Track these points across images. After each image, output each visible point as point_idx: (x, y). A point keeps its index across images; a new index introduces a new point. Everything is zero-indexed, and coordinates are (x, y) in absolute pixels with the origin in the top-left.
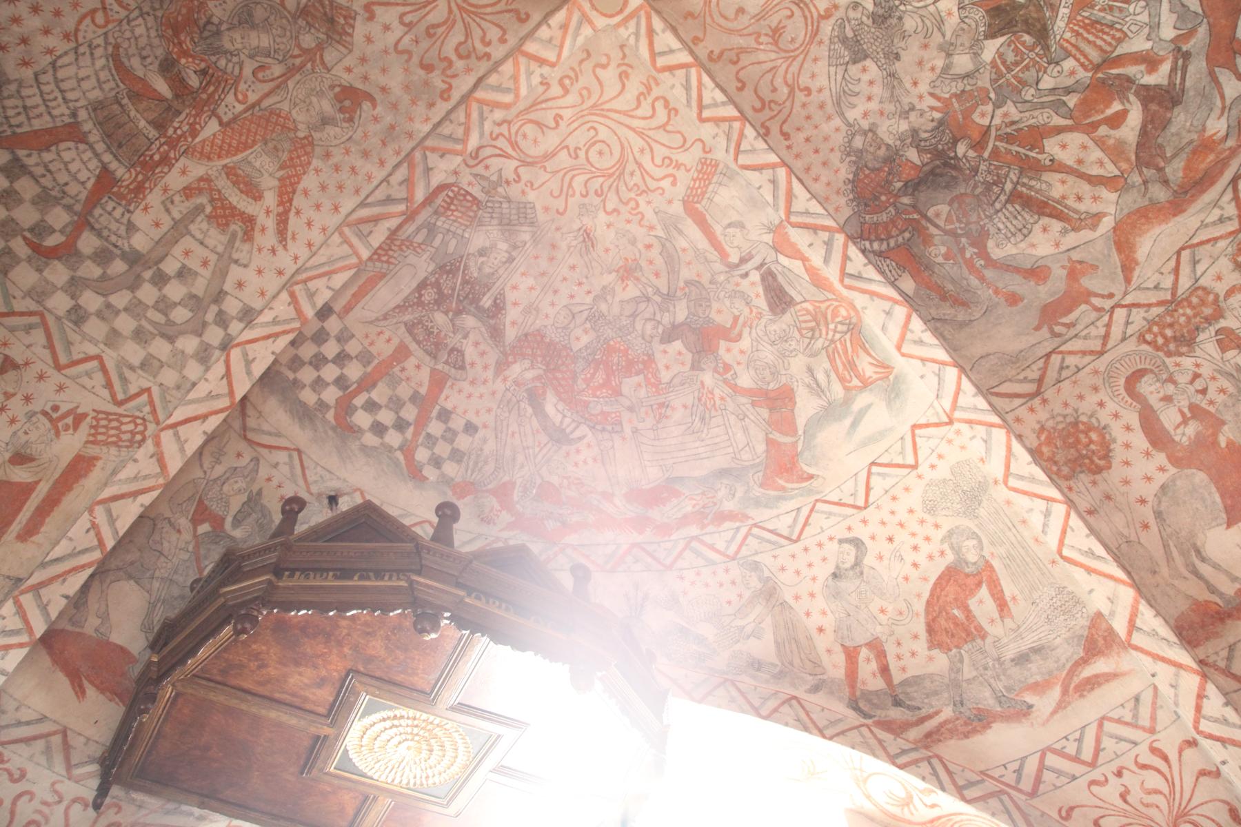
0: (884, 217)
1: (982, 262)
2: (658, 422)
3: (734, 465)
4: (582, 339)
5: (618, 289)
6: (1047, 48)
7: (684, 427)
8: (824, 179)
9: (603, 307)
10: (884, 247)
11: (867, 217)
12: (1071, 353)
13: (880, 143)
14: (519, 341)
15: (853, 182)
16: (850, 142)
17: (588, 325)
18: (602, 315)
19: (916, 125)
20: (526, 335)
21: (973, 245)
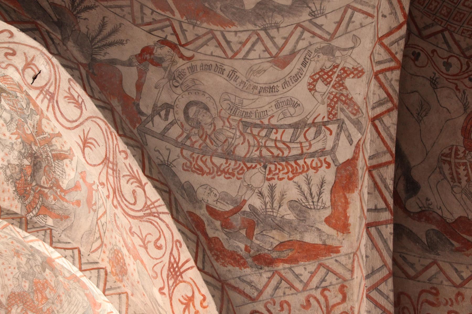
0: (31, 197)
1: (63, 194)
2: (61, 304)
3: (85, 310)
4: (26, 285)
5: (20, 261)
6: (10, 94)
7: (67, 302)
8: (6, 198)
9: (23, 270)
10: (37, 210)
11: (26, 202)
12: (101, 217)
13: (14, 166)
14: (8, 300)
15: (16, 190)
16: (6, 175)
17: (24, 279)
18: (25, 273)
19: (18, 149)
20: (9, 297)
21: (57, 188)
